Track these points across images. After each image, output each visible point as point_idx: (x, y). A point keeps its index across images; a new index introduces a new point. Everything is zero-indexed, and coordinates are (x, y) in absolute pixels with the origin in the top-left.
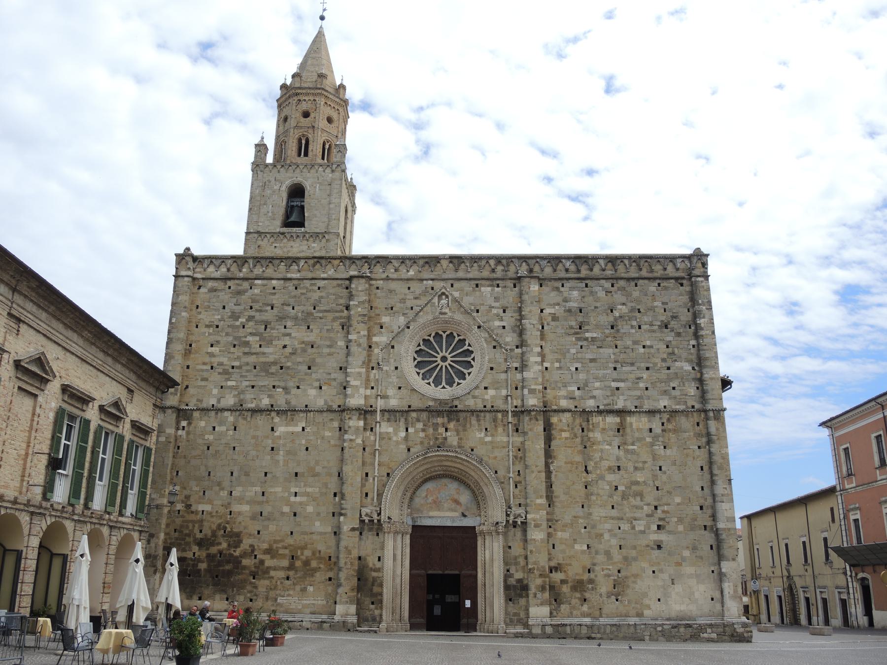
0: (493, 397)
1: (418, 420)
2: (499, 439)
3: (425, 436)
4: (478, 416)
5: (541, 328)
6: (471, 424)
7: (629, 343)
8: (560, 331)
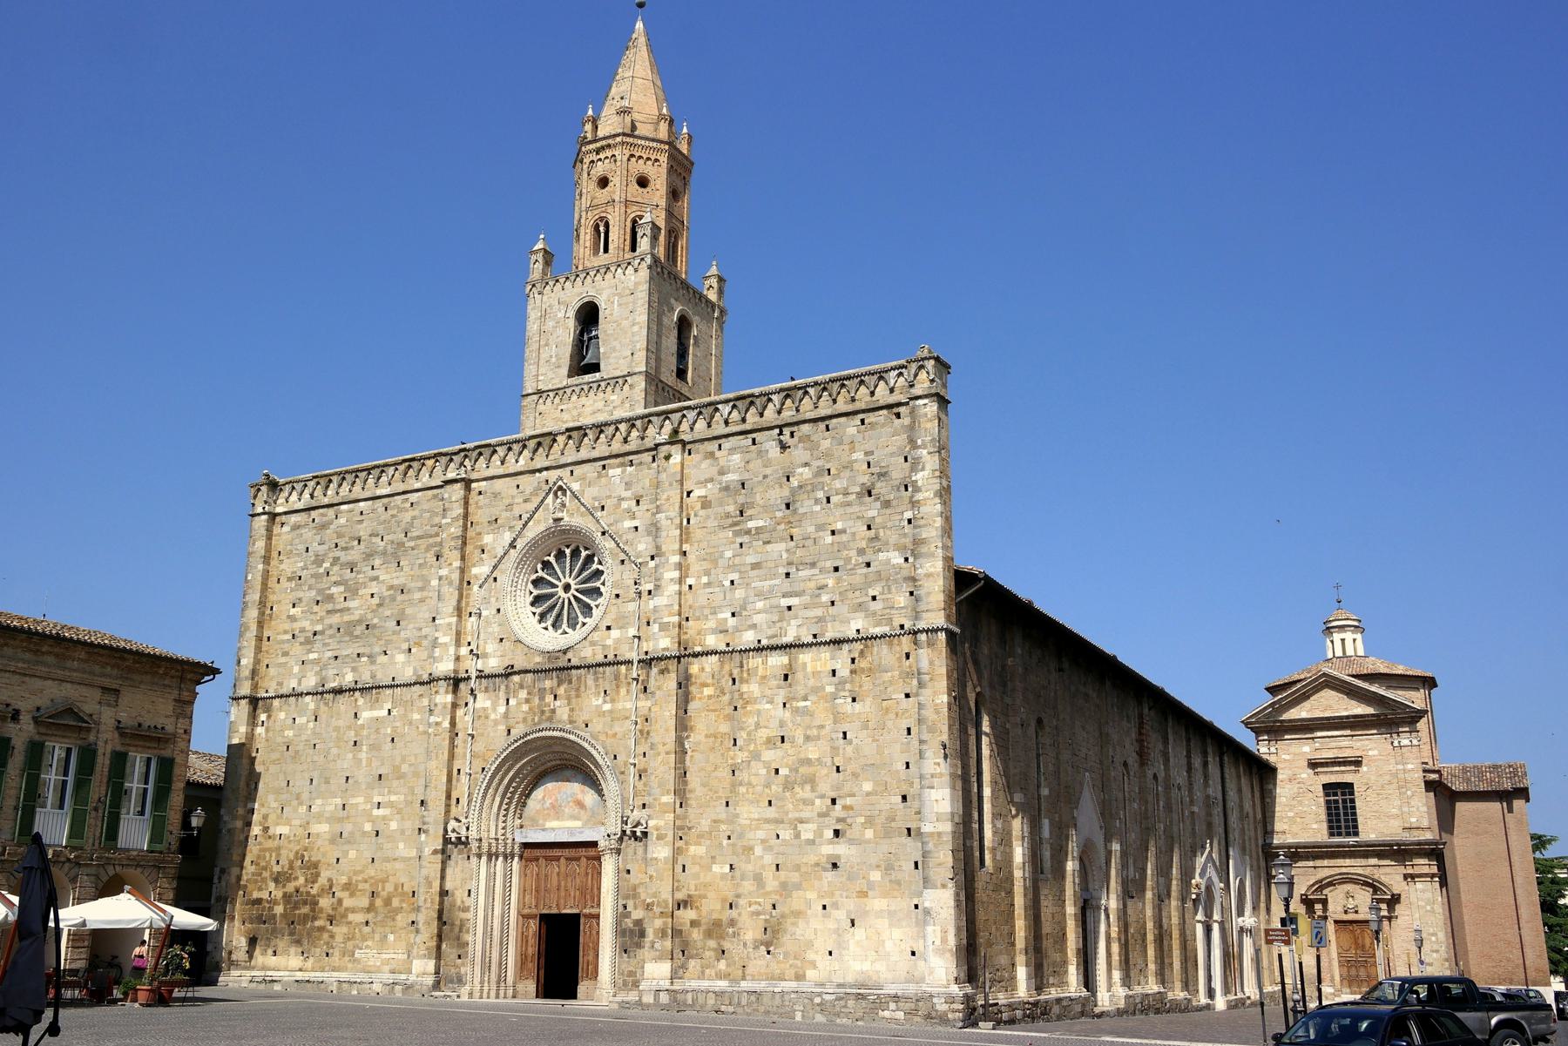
0: (618, 641)
1: (521, 687)
2: (620, 706)
3: (530, 709)
4: (595, 673)
7: (811, 529)
8: (712, 523)
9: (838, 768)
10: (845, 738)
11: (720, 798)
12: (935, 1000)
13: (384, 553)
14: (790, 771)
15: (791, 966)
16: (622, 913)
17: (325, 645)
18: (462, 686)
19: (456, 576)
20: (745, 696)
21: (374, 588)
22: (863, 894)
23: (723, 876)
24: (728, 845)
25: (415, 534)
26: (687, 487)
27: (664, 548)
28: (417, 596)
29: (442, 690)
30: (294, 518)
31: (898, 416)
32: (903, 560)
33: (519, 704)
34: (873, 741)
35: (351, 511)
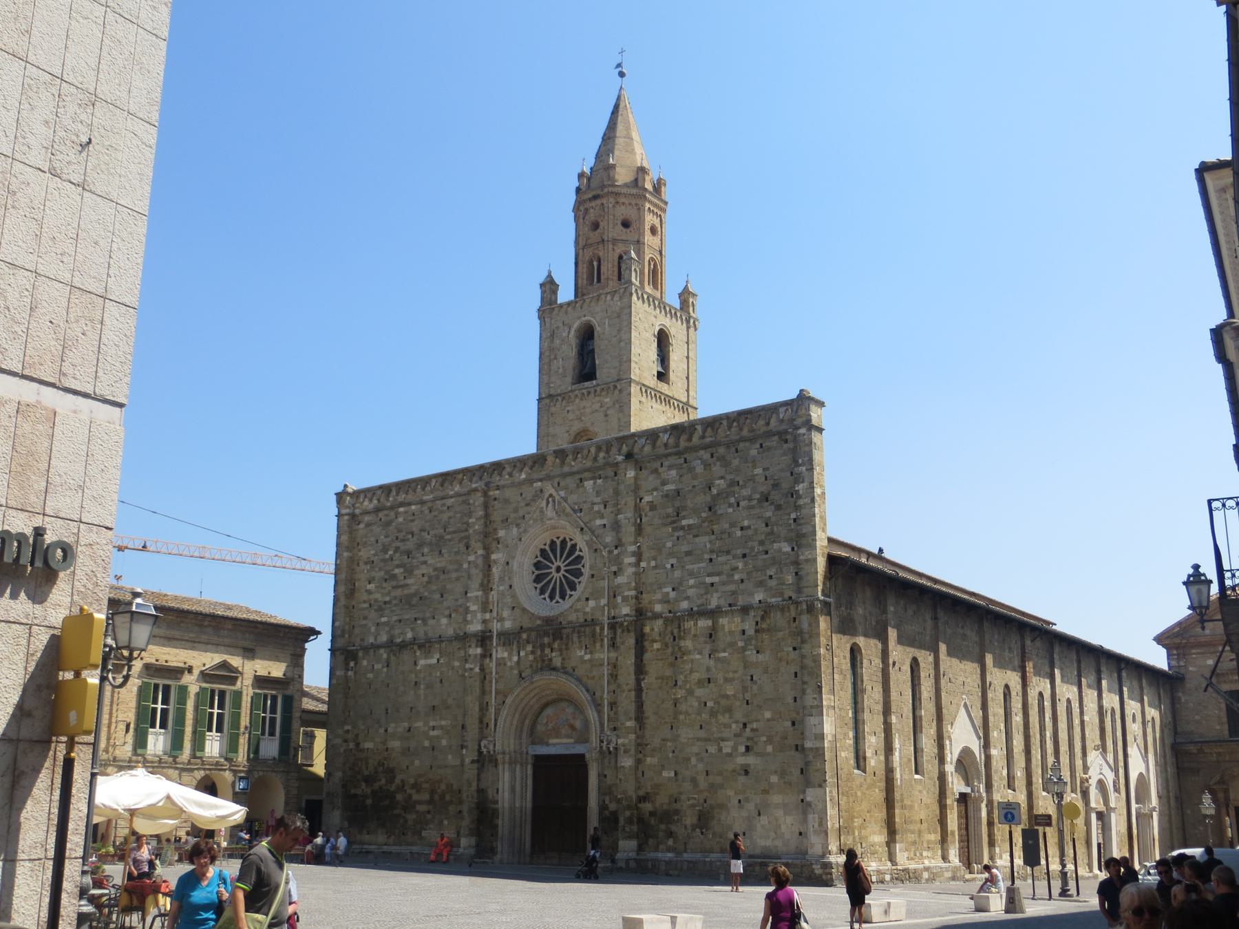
0: (593, 609)
1: (528, 642)
2: (597, 656)
5: (639, 521)
6: (572, 642)
7: (726, 526)
9: (747, 701)
10: (752, 680)
11: (666, 723)
12: (814, 866)
13: (430, 544)
14: (715, 704)
15: (718, 843)
16: (603, 807)
17: (393, 611)
18: (488, 643)
19: (480, 561)
20: (683, 649)
21: (424, 570)
22: (765, 792)
23: (670, 779)
24: (673, 756)
25: (451, 530)
26: (641, 494)
27: (623, 540)
28: (454, 575)
29: (473, 645)
30: (367, 518)
31: (786, 441)
32: (789, 549)
33: (526, 655)
34: (772, 681)
35: (406, 512)
